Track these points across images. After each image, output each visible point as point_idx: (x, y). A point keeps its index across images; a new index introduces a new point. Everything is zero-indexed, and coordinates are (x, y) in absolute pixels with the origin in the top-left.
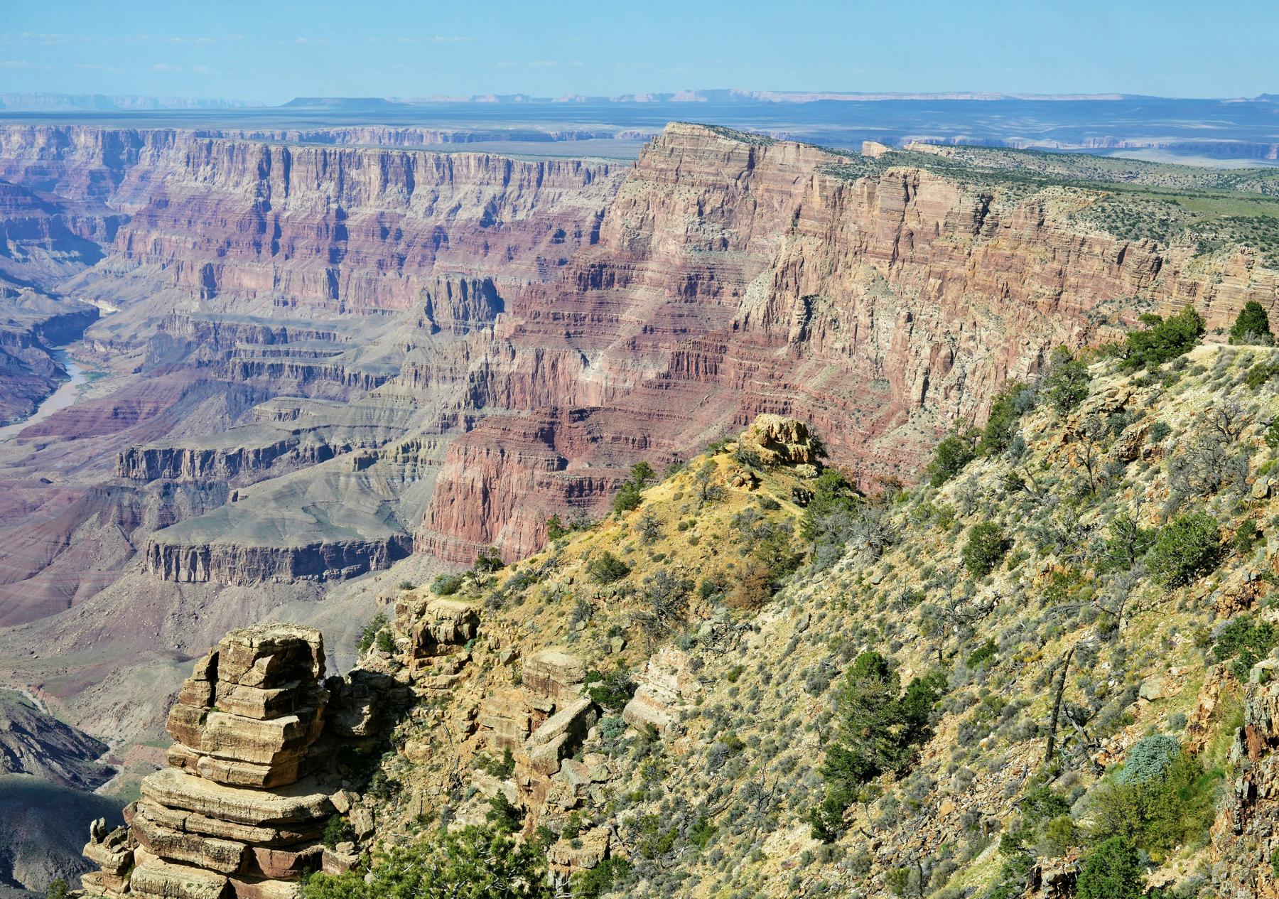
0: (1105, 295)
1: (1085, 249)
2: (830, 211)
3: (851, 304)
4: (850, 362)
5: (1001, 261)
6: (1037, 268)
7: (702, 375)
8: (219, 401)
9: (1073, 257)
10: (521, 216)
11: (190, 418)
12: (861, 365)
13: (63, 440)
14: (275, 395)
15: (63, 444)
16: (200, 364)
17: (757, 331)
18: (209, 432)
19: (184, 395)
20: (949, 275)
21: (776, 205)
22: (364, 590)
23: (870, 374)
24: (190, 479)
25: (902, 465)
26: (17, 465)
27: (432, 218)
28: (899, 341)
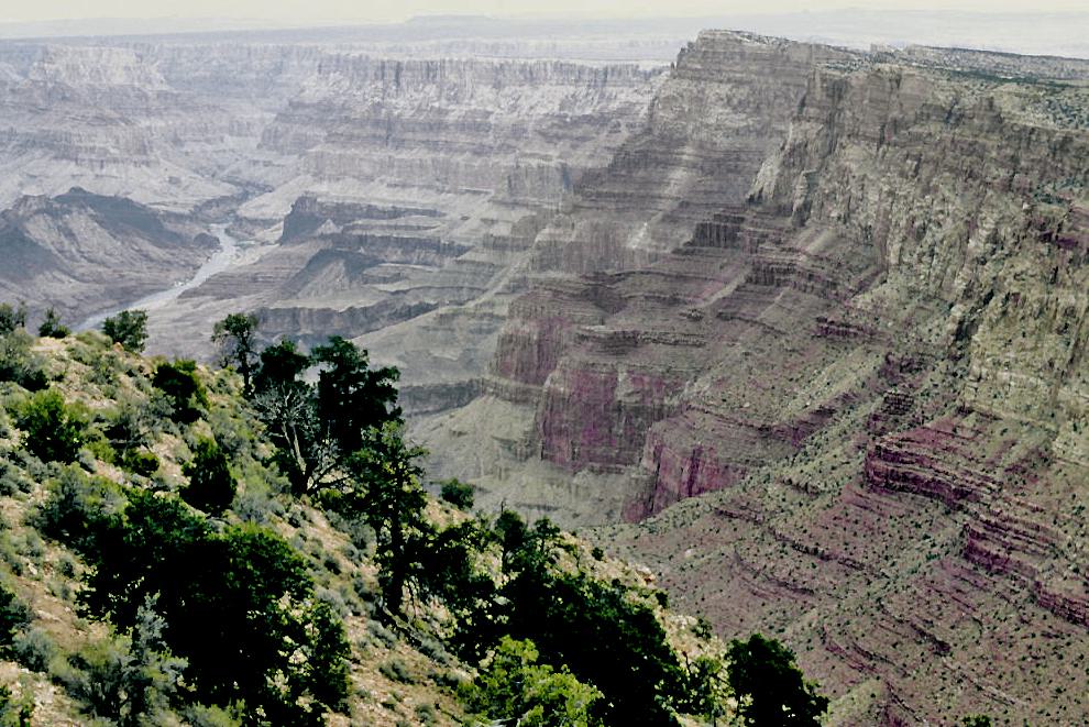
0: (1049, 177)
1: (1034, 137)
2: (830, 100)
3: (845, 179)
4: (844, 227)
5: (965, 147)
6: (994, 154)
7: (722, 243)
8: (340, 266)
9: (1024, 144)
10: (588, 111)
11: (315, 282)
12: (854, 231)
13: (215, 300)
14: (384, 262)
15: (214, 304)
16: (323, 237)
17: (768, 203)
18: (330, 292)
19: (310, 262)
20: (923, 158)
21: (793, 96)
22: (441, 425)
23: (861, 240)
24: (309, 332)
25: (881, 319)
26: (174, 321)
27: (515, 114)
28: (882, 212)
